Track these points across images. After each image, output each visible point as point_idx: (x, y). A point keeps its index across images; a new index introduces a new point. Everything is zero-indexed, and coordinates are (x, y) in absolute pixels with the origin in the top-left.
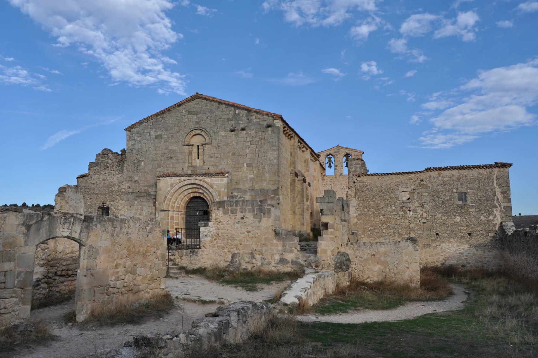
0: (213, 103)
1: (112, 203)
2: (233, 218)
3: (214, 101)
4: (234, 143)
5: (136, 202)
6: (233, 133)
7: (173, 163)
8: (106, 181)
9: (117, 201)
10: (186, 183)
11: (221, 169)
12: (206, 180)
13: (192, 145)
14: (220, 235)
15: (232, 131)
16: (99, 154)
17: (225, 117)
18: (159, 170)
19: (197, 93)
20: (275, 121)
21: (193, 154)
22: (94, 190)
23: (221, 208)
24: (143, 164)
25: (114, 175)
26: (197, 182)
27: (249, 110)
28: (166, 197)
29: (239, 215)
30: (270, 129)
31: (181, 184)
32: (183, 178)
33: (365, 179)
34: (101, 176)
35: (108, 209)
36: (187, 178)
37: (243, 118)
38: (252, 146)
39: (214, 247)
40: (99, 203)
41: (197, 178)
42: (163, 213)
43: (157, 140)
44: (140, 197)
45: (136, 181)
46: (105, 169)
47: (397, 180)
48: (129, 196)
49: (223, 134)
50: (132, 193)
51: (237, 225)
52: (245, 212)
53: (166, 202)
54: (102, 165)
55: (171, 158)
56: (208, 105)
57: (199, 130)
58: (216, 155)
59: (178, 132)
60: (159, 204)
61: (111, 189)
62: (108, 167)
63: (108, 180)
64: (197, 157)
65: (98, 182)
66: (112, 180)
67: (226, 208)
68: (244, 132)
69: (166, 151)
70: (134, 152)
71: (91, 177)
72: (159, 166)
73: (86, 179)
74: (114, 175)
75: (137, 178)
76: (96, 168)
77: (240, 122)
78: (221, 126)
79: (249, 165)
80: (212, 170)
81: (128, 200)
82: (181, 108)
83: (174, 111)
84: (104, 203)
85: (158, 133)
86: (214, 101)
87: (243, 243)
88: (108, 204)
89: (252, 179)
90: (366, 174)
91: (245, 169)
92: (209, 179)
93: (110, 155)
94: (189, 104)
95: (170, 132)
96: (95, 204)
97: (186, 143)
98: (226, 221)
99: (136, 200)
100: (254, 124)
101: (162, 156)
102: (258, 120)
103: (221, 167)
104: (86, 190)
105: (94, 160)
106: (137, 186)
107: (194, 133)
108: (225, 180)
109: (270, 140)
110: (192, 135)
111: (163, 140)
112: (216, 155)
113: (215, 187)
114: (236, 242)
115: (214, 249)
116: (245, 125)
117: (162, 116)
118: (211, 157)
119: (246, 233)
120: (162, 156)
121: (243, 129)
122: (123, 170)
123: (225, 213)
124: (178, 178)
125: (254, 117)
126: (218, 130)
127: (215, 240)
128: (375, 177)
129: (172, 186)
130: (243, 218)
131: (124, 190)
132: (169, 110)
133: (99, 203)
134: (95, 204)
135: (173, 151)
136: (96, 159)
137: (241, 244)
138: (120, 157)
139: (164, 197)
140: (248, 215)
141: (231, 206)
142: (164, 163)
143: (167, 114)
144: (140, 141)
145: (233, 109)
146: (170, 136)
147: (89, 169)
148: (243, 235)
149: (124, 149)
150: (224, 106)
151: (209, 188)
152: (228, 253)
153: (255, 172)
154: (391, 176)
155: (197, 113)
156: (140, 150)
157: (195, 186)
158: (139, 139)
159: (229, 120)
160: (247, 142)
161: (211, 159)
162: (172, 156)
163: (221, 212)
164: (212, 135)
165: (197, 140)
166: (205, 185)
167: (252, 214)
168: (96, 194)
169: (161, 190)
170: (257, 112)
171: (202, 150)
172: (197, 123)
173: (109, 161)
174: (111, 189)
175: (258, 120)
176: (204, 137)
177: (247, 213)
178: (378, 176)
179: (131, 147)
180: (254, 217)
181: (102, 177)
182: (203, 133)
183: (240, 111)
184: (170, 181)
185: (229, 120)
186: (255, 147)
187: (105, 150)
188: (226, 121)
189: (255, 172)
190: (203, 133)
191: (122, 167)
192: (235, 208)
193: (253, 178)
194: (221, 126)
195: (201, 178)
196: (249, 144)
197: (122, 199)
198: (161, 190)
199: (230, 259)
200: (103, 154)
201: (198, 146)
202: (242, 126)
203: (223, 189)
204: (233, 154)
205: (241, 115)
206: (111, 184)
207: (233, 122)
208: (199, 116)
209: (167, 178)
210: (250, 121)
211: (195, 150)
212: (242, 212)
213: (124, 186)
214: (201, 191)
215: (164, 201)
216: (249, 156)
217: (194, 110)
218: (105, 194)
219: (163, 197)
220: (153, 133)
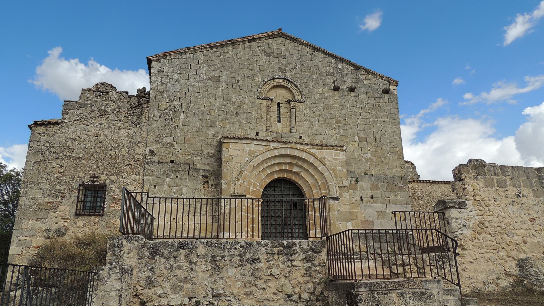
0: (304, 47)
1: (112, 178)
2: (504, 194)
3: (308, 45)
4: (338, 106)
5: (168, 179)
6: (336, 92)
7: (240, 122)
8: (102, 137)
9: (125, 175)
10: (276, 153)
11: (321, 141)
12: (311, 150)
13: (272, 100)
14: (487, 224)
15: (336, 89)
16: (89, 90)
17: (323, 69)
18: (214, 129)
19: (280, 30)
20: (391, 87)
21: (272, 114)
23: (480, 177)
24: (182, 116)
25: (120, 128)
26: (296, 153)
27: (357, 67)
28: (241, 172)
29: (512, 191)
30: (386, 96)
31: (269, 155)
32: (272, 145)
33: (416, 185)
34: (91, 127)
35: (103, 188)
36: (280, 145)
37: (349, 76)
38: (364, 114)
39: (481, 248)
40: (81, 175)
41: (299, 146)
43: (210, 83)
44: (178, 171)
45: (168, 143)
47: (446, 190)
48: (154, 168)
49: (321, 91)
50: (159, 163)
51: (511, 209)
52: (520, 186)
53: (241, 181)
54: (94, 108)
55: (237, 114)
56: (296, 48)
57: (283, 82)
58: (312, 120)
59: (248, 77)
60: (228, 184)
61: (112, 153)
62: (107, 113)
63: (106, 136)
64: (277, 119)
65: (83, 137)
66: (115, 136)
67: (487, 176)
68: (352, 94)
69: (228, 103)
70: (165, 94)
72: (214, 124)
73: (54, 128)
74: (120, 128)
75: (169, 139)
76: (80, 111)
77: (345, 79)
78: (318, 80)
79: (361, 140)
80: (306, 139)
81: (152, 175)
82: (253, 44)
83: (242, 46)
85: (213, 74)
86: (308, 45)
87: (528, 240)
88: (103, 178)
89: (368, 160)
90: (417, 180)
91: (357, 145)
92: (317, 151)
93: (113, 95)
94: (268, 41)
95: (234, 74)
96: (73, 177)
97: (263, 95)
98: (492, 200)
99: (168, 176)
100: (365, 85)
101: (219, 109)
102: (369, 82)
103: (320, 137)
104: (53, 150)
105: (77, 99)
106: (169, 153)
107: (274, 83)
108: (342, 155)
109: (388, 110)
110: (272, 85)
111: (222, 85)
112: (312, 120)
113: (327, 163)
114: (516, 238)
115: (483, 251)
116: (353, 85)
117: (221, 49)
118: (305, 121)
119: (529, 222)
120: (219, 109)
121: (352, 90)
122: (139, 123)
123: (488, 185)
124: (264, 143)
125: (364, 76)
126: (313, 85)
127: (480, 234)
128: (426, 185)
129: (252, 155)
130: (519, 196)
131: (141, 157)
132: (233, 43)
133: (81, 175)
134: (73, 177)
135: (241, 105)
136: (80, 98)
137: (525, 242)
138: (135, 101)
140: (525, 191)
141: (495, 175)
142: (223, 119)
143: (230, 48)
144: (177, 80)
145: (334, 60)
146: (234, 82)
147: (64, 113)
148: (525, 226)
149: (144, 88)
150: (321, 55)
151: (317, 164)
152: (507, 259)
153: (371, 150)
154: (441, 185)
155: (281, 57)
156: (177, 94)
157: (288, 160)
158: (176, 77)
159: (328, 74)
160: (357, 108)
161: (304, 124)
162: (238, 111)
163: (482, 184)
165: (279, 95)
166: (311, 160)
167: (531, 190)
168: (75, 158)
169: (230, 160)
170: (367, 71)
171: (287, 110)
172: (280, 70)
173: (111, 103)
174: (112, 153)
175: (369, 82)
177: (522, 188)
178: (429, 184)
179: (159, 87)
180: (535, 196)
181: (92, 129)
182: (290, 86)
183: (344, 65)
184: (248, 147)
185: (328, 74)
186: (368, 116)
187: (102, 84)
188: (325, 74)
189: (371, 150)
190: (290, 86)
191: (140, 116)
192: (501, 177)
193: (370, 158)
194: (318, 80)
196: (360, 110)
197: (137, 174)
198: (230, 160)
199: (515, 270)
200: (98, 90)
201: (279, 104)
202: (349, 85)
203: (340, 168)
204: (338, 122)
205: (346, 72)
206: (113, 143)
207: (335, 79)
208: (282, 60)
209: (244, 141)
210: (359, 81)
211: (275, 108)
212: (514, 186)
213: (141, 151)
214: (295, 169)
215: (238, 179)
216: (361, 127)
217: (275, 51)
218: (98, 161)
219: (235, 174)
220: (203, 72)
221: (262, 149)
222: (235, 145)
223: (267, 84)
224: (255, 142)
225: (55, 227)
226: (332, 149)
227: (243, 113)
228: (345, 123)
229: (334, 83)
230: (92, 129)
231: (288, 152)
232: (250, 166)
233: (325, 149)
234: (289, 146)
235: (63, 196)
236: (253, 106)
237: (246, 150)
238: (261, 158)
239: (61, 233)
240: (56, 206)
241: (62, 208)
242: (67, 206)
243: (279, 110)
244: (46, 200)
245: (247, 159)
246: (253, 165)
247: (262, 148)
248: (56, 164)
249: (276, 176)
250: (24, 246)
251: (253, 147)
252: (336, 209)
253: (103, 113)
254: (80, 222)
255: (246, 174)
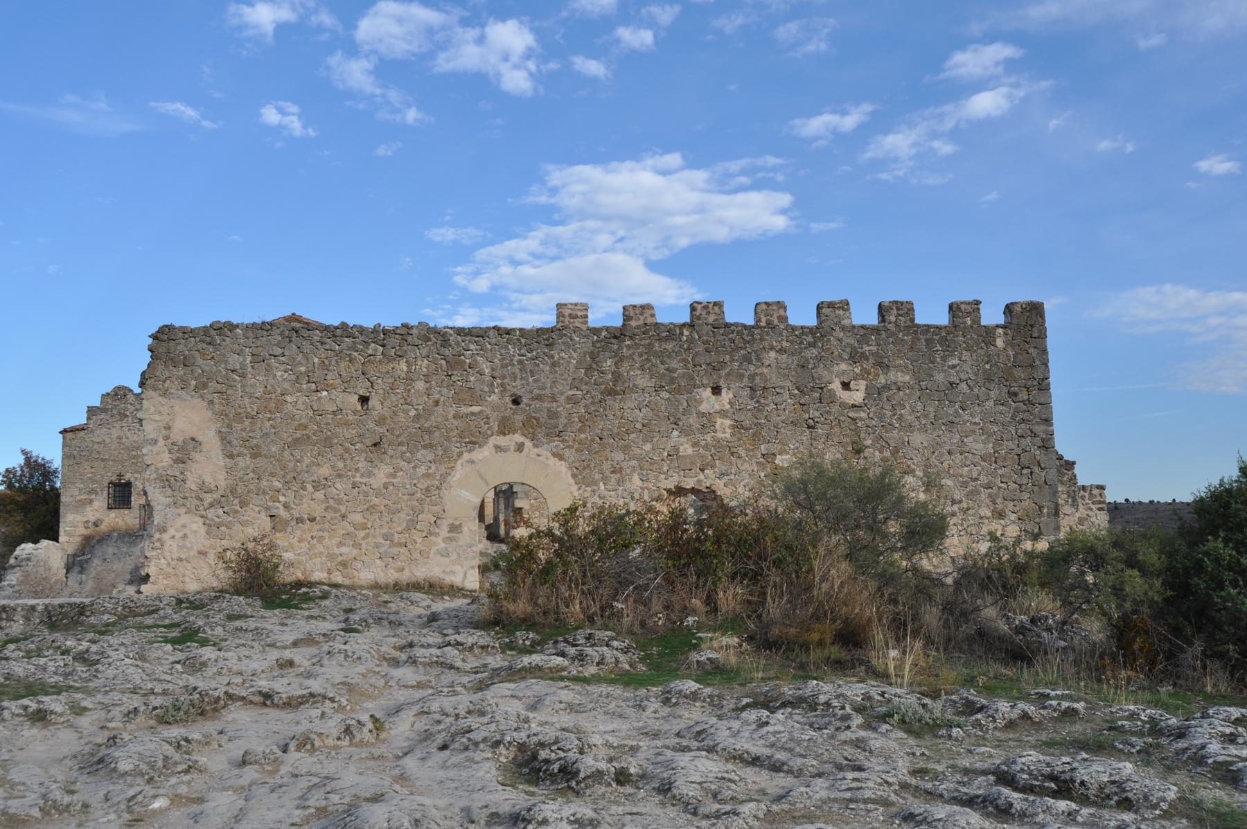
22: (99, 453)
34: (113, 431)
46: (121, 420)
62: (126, 416)
65: (108, 441)
66: (135, 438)
71: (92, 431)
73: (82, 434)
84: (120, 475)
88: (128, 476)
96: (102, 477)
105: (98, 404)
134: (102, 477)
147: (88, 419)
168: (103, 460)
181: (115, 432)
187: (119, 388)
225: (92, 519)
230: (115, 432)
235: (96, 493)
239: (96, 524)
240: (91, 501)
241: (96, 504)
242: (100, 502)
244: (83, 497)
248: (86, 466)
250: (69, 535)
253: (123, 416)
254: (113, 514)
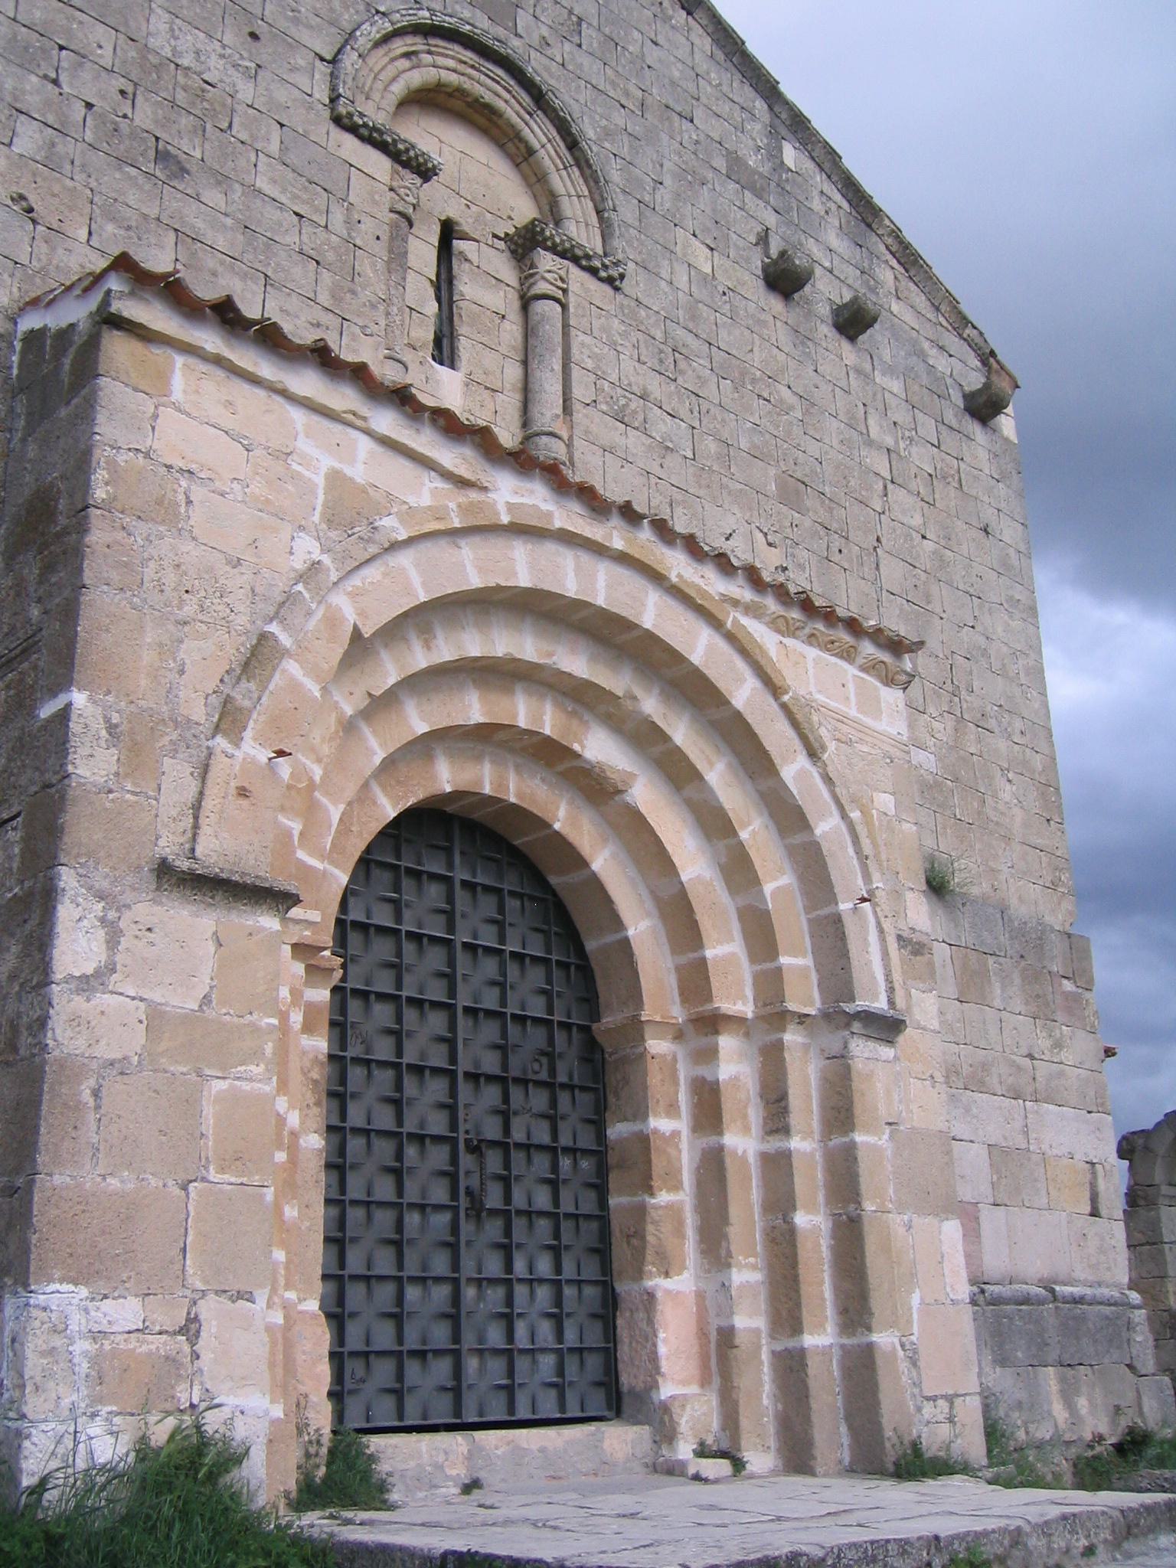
10: (522, 566)
26: (652, 612)
28: (259, 657)
31: (471, 568)
36: (567, 516)
42: (196, 924)
124: (453, 457)
135: (207, 107)
139: (232, 648)
151: (775, 734)
157: (575, 662)
162: (189, 148)
164: (626, 211)
166: (744, 693)
169: (167, 512)
171: (504, 300)
176: (535, 180)
182: (538, 133)
190: (538, 133)
195: (711, 583)
201: (448, 232)
219: (205, 660)
221: (426, 500)
222: (215, 388)
223: (399, 46)
224: (386, 421)
226: (848, 655)
227: (222, 180)
228: (823, 515)
229: (763, 239)
231: (601, 586)
232: (332, 620)
233: (812, 639)
234: (618, 544)
236: (292, 158)
237: (307, 461)
238: (416, 579)
243: (444, 285)
245: (307, 548)
246: (350, 616)
247: (425, 492)
249: (445, 776)
251: (363, 462)
252: (883, 1112)
255: (294, 687)
